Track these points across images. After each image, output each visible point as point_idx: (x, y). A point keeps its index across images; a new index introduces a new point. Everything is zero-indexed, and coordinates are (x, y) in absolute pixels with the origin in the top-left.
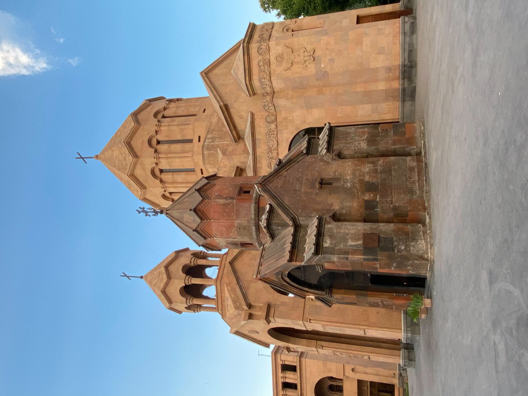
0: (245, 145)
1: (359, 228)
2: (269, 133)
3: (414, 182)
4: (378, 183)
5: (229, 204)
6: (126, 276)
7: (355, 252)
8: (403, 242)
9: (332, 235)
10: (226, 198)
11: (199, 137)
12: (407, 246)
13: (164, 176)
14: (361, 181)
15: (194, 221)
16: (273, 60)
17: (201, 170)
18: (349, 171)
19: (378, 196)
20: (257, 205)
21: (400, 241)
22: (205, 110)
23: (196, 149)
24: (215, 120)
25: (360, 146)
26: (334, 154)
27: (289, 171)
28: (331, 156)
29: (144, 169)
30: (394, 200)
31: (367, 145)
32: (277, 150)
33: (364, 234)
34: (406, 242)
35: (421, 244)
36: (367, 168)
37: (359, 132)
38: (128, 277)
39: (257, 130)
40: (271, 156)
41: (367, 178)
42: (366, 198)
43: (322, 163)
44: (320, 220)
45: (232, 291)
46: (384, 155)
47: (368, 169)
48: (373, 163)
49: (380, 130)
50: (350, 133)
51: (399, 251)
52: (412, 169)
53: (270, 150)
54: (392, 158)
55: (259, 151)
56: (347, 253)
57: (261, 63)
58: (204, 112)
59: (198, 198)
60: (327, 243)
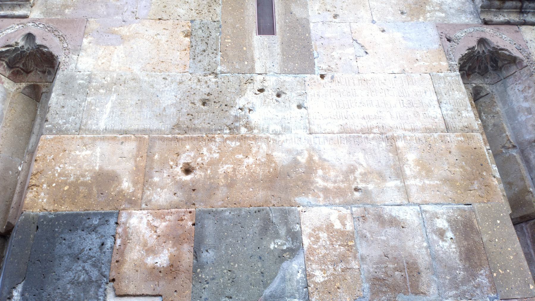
14: (289, 180)
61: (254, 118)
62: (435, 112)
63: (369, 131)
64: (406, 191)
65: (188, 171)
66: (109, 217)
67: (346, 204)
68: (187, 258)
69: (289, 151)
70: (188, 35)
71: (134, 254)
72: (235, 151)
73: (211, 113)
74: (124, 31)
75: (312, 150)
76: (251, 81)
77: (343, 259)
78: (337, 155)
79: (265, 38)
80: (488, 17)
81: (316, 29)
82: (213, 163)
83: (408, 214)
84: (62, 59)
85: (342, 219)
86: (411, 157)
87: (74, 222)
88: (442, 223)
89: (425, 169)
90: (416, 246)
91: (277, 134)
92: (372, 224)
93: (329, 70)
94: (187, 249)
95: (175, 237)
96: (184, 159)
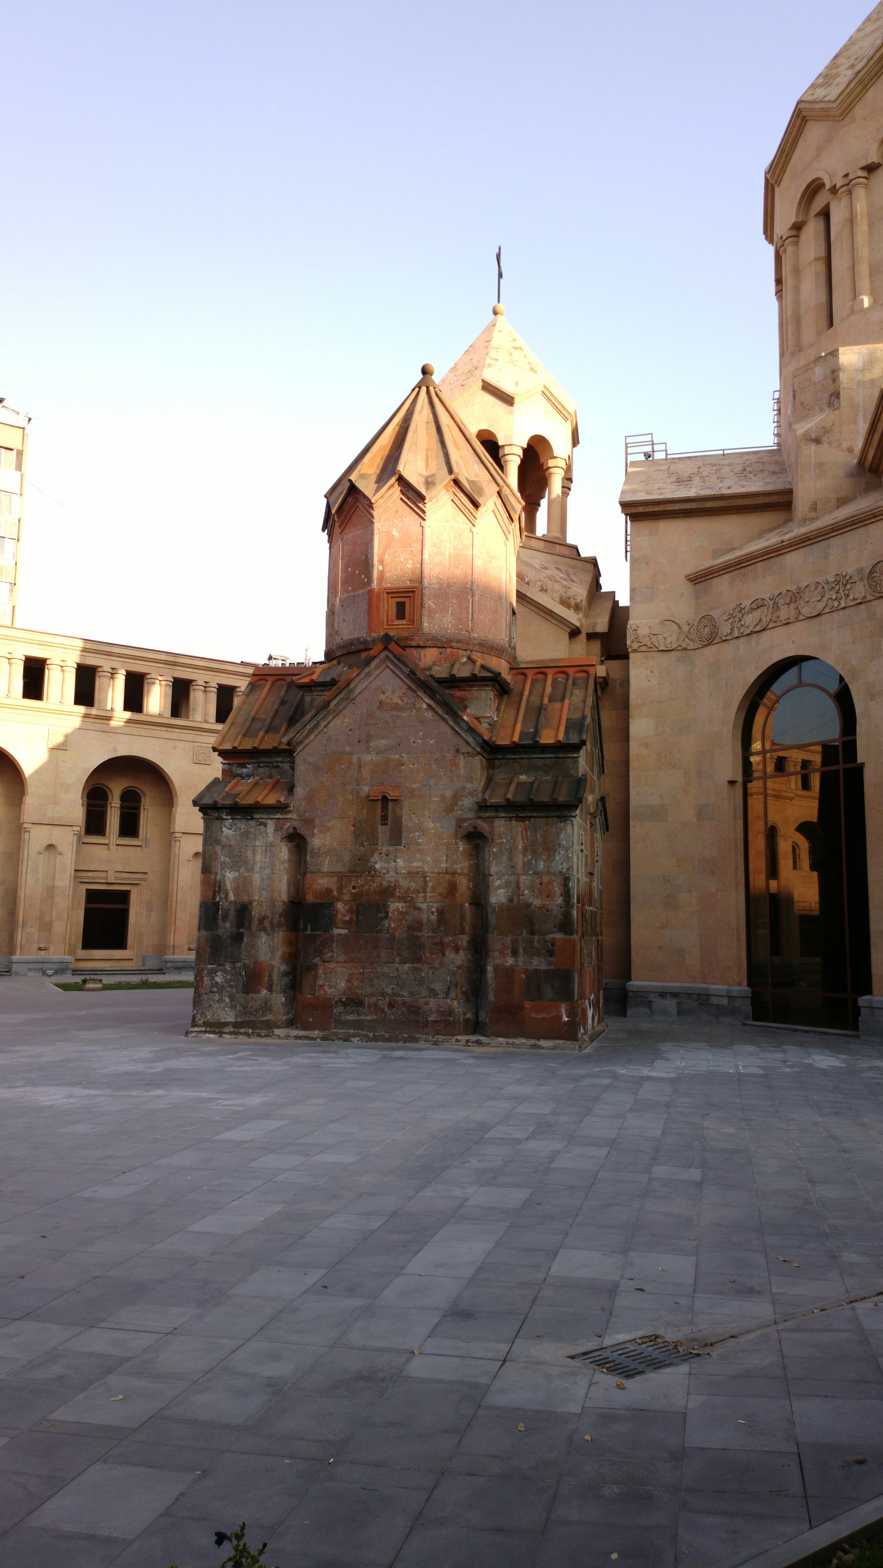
0: (842, 502)
1: (264, 892)
2: (843, 582)
4: (380, 931)
8: (231, 980)
9: (247, 838)
10: (381, 562)
14: (388, 892)
18: (419, 864)
19: (343, 932)
20: (362, 647)
21: (232, 975)
25: (499, 887)
26: (479, 822)
27: (429, 715)
28: (471, 815)
30: (332, 965)
31: (501, 906)
32: (797, 620)
33: (251, 903)
34: (230, 986)
37: (550, 882)
39: (854, 538)
40: (781, 601)
41: (396, 906)
42: (340, 906)
43: (449, 794)
44: (281, 808)
46: (479, 949)
49: (552, 936)
50: (550, 859)
51: (212, 973)
53: (795, 597)
55: (793, 559)
60: (228, 830)
61: (377, 866)
62: (444, 865)
63: (417, 873)
64: (425, 898)
65: (354, 888)
66: (331, 905)
67: (405, 902)
68: (355, 919)
69: (388, 881)
70: (354, 826)
71: (339, 916)
72: (370, 881)
73: (361, 866)
74: (330, 825)
75: (396, 881)
76: (376, 849)
77: (401, 920)
78: (404, 883)
79: (384, 827)
80: (482, 814)
81: (405, 820)
82: (362, 886)
83: (424, 906)
84: (308, 840)
85: (402, 907)
86: (430, 884)
87: (321, 905)
88: (434, 910)
89: (434, 889)
90: (424, 917)
91: (384, 874)
92: (412, 909)
93: (407, 844)
94: (354, 915)
95: (350, 911)
96: (353, 884)
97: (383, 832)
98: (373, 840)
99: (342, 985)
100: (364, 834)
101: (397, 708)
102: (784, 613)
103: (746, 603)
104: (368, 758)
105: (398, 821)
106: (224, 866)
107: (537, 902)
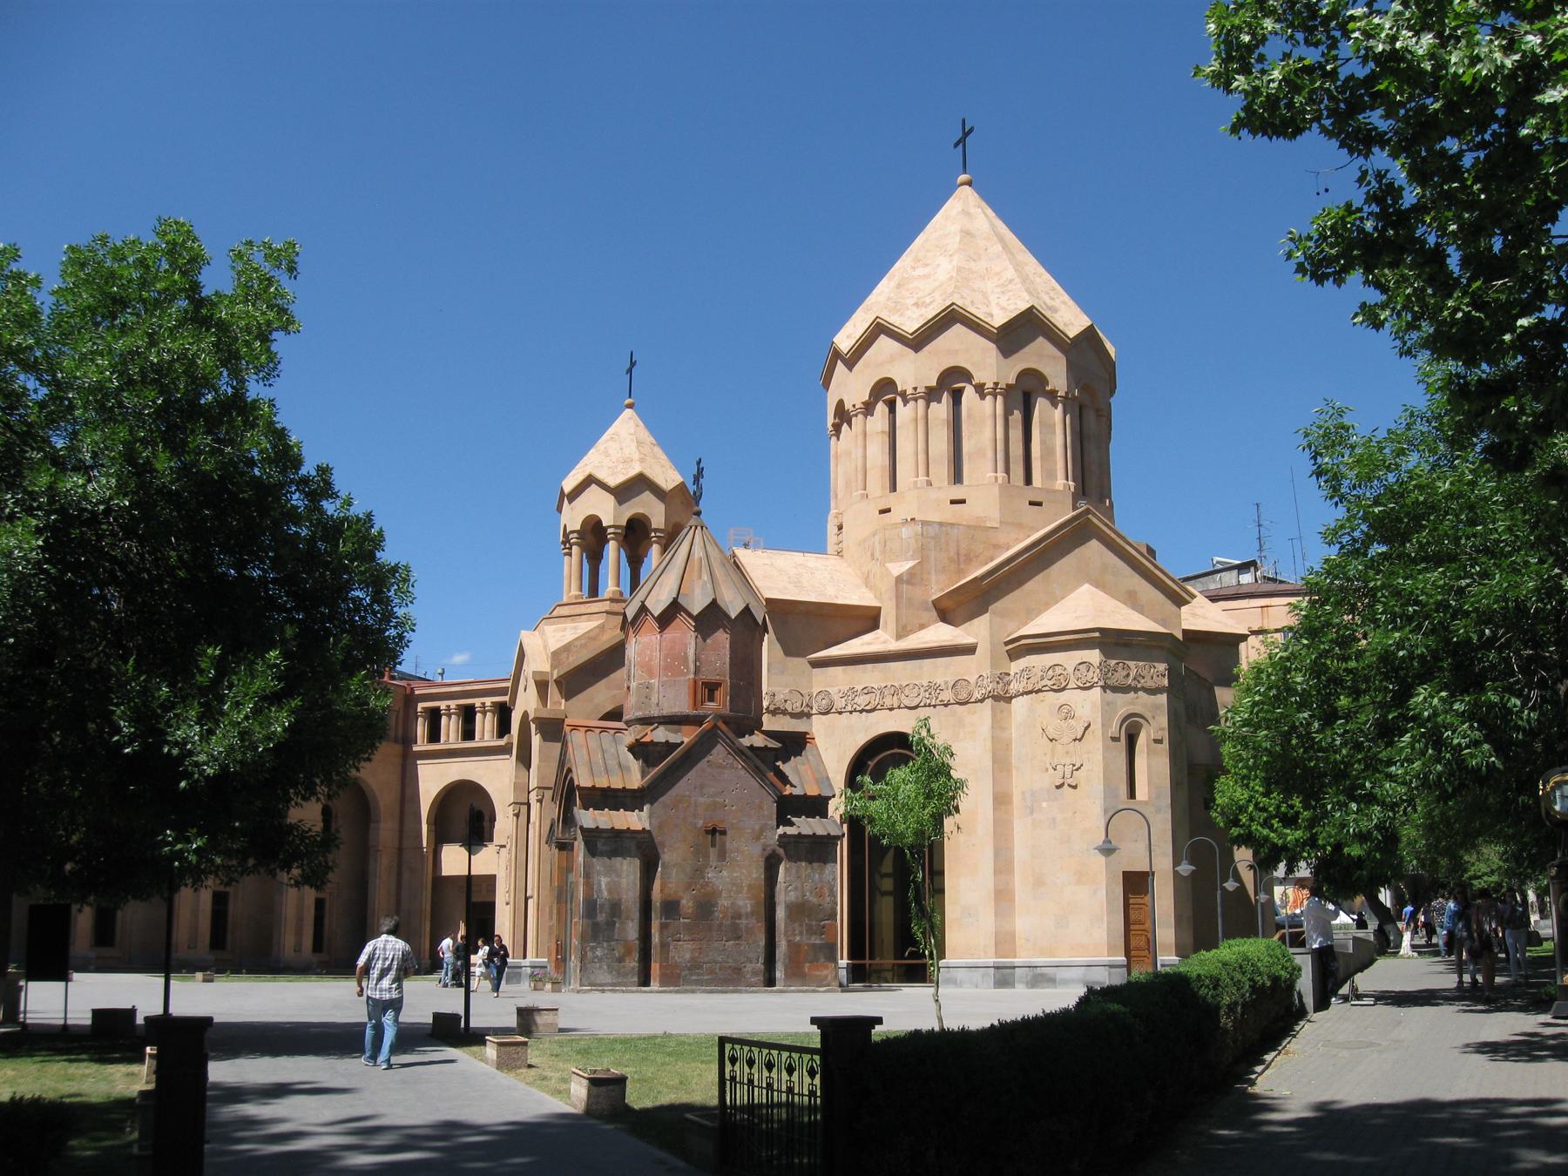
0: (922, 627)
2: (934, 688)
3: (712, 972)
5: (687, 667)
6: (633, 364)
7: (589, 885)
11: (963, 502)
12: (600, 960)
13: (881, 408)
15: (658, 601)
16: (1064, 697)
17: (889, 510)
22: (1039, 504)
23: (933, 494)
24: (1002, 538)
29: (892, 359)
35: (606, 977)
36: (746, 904)
38: (630, 371)
41: (724, 902)
42: (684, 902)
45: (589, 637)
47: (740, 903)
48: (752, 913)
51: (593, 949)
52: (738, 970)
54: (762, 943)
56: (587, 876)
57: (1058, 670)
58: (1031, 503)
59: (697, 605)
97: (713, 852)
98: (706, 856)
99: (688, 956)
100: (699, 852)
101: (720, 766)
102: (888, 702)
103: (859, 688)
104: (702, 800)
105: (723, 845)
106: (599, 873)
107: (814, 900)
